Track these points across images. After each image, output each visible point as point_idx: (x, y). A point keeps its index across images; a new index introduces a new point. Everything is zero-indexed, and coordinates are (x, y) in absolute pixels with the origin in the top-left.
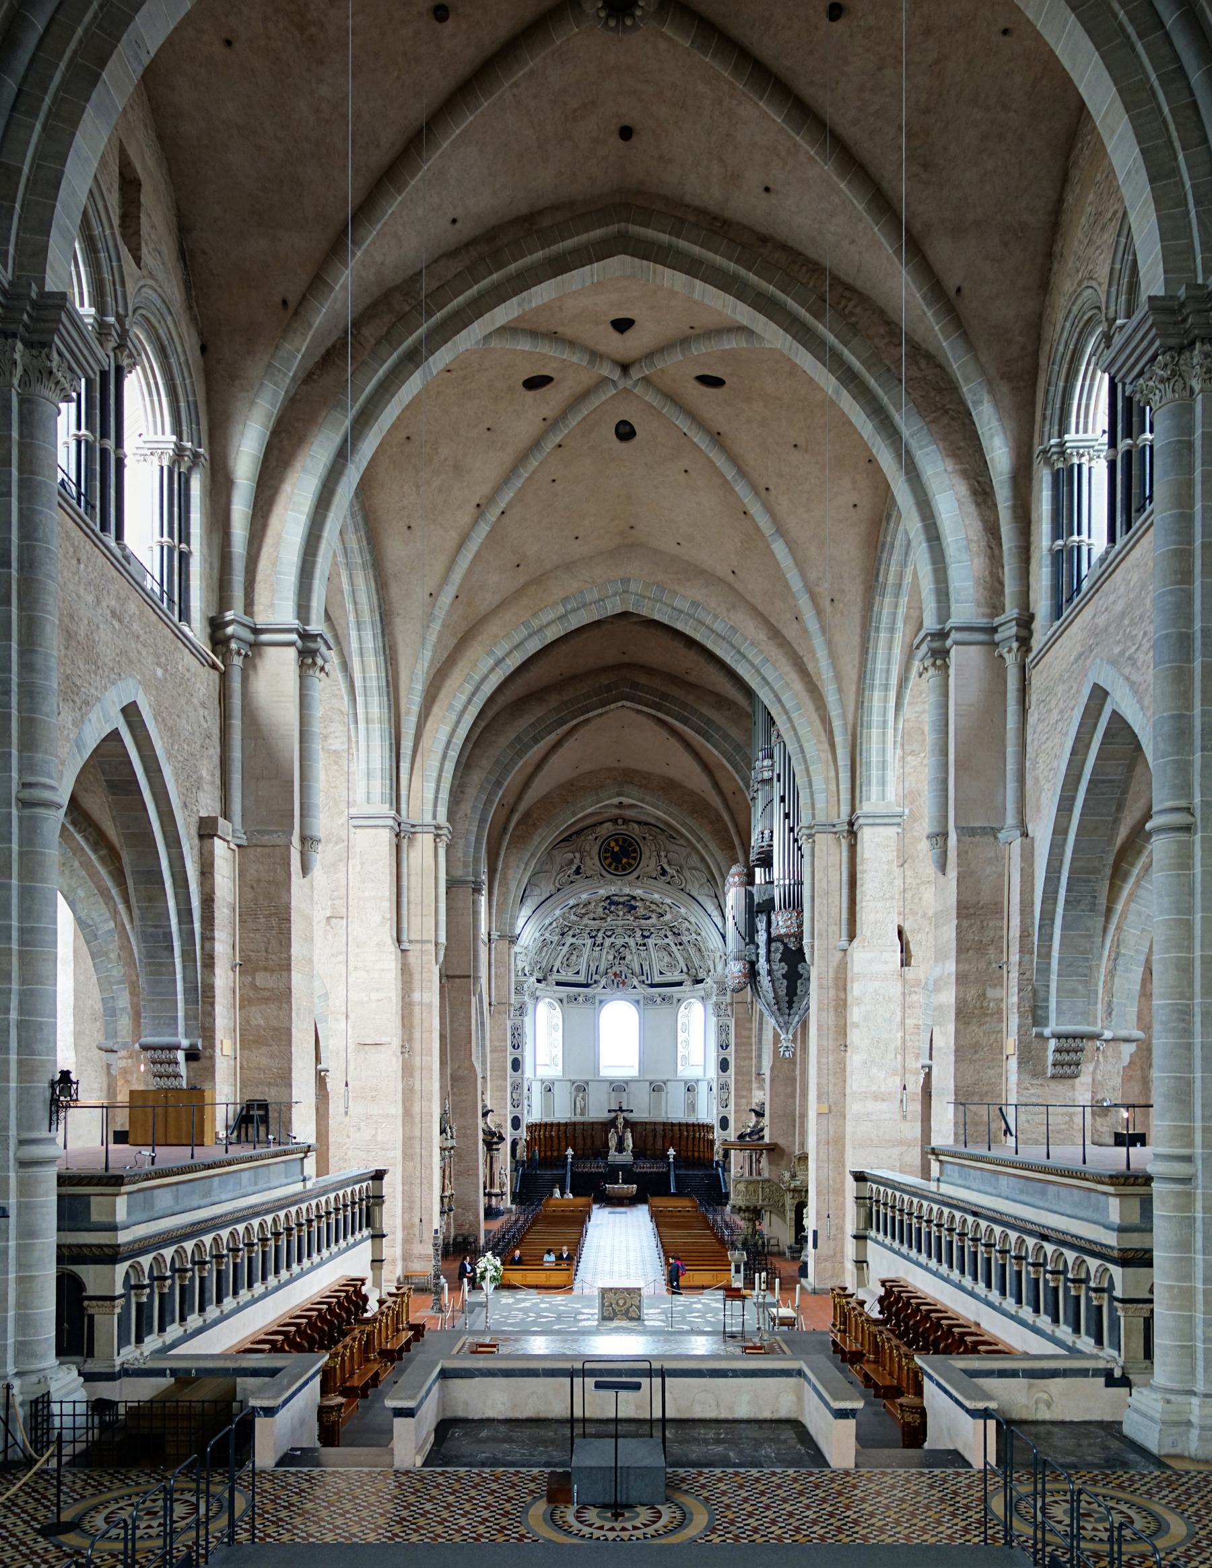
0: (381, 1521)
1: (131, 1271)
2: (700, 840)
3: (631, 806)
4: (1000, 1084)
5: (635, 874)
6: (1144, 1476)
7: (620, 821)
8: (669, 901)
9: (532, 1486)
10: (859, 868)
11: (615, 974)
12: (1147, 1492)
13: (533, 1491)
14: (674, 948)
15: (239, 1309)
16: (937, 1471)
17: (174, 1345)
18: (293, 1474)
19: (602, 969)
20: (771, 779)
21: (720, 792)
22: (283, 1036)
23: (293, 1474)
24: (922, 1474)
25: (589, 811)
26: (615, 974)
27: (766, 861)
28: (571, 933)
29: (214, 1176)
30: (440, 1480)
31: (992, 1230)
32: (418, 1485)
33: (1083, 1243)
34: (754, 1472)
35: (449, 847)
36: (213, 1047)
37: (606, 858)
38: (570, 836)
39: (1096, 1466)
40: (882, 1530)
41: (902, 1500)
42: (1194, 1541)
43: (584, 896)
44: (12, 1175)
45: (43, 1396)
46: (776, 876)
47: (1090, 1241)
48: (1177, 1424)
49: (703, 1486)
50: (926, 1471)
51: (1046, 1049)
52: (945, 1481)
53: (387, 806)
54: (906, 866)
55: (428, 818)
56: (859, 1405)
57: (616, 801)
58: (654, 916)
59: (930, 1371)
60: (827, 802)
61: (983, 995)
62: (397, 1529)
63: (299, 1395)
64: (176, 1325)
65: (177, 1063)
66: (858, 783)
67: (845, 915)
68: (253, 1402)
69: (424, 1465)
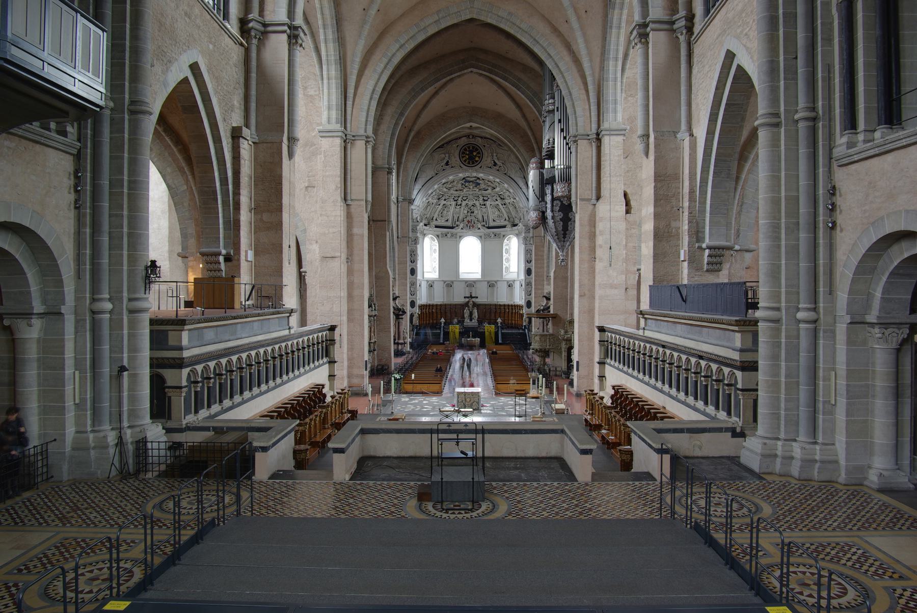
0: (324, 508)
1: (191, 373)
3: (476, 128)
5: (479, 165)
6: (751, 484)
7: (471, 137)
8: (498, 180)
9: (410, 491)
10: (602, 159)
11: (468, 222)
12: (751, 492)
13: (410, 494)
14: (501, 207)
16: (637, 483)
18: (278, 483)
19: (461, 218)
20: (554, 110)
22: (277, 249)
23: (278, 483)
24: (629, 485)
25: (453, 131)
26: (468, 222)
27: (551, 156)
28: (443, 198)
29: (238, 323)
30: (359, 487)
32: (346, 490)
33: (721, 359)
34: (535, 484)
35: (374, 149)
37: (463, 157)
38: (443, 145)
39: (725, 479)
40: (604, 513)
41: (616, 498)
42: (776, 517)
43: (451, 178)
46: (556, 163)
48: (770, 456)
49: (506, 491)
50: (631, 483)
51: (704, 255)
52: (641, 488)
53: (339, 125)
54: (628, 158)
55: (362, 132)
56: (593, 447)
57: (468, 125)
58: (490, 188)
59: (635, 429)
61: (669, 225)
62: (333, 512)
63: (282, 442)
65: (220, 263)
66: (601, 112)
67: (594, 185)
68: (255, 444)
69: (350, 480)
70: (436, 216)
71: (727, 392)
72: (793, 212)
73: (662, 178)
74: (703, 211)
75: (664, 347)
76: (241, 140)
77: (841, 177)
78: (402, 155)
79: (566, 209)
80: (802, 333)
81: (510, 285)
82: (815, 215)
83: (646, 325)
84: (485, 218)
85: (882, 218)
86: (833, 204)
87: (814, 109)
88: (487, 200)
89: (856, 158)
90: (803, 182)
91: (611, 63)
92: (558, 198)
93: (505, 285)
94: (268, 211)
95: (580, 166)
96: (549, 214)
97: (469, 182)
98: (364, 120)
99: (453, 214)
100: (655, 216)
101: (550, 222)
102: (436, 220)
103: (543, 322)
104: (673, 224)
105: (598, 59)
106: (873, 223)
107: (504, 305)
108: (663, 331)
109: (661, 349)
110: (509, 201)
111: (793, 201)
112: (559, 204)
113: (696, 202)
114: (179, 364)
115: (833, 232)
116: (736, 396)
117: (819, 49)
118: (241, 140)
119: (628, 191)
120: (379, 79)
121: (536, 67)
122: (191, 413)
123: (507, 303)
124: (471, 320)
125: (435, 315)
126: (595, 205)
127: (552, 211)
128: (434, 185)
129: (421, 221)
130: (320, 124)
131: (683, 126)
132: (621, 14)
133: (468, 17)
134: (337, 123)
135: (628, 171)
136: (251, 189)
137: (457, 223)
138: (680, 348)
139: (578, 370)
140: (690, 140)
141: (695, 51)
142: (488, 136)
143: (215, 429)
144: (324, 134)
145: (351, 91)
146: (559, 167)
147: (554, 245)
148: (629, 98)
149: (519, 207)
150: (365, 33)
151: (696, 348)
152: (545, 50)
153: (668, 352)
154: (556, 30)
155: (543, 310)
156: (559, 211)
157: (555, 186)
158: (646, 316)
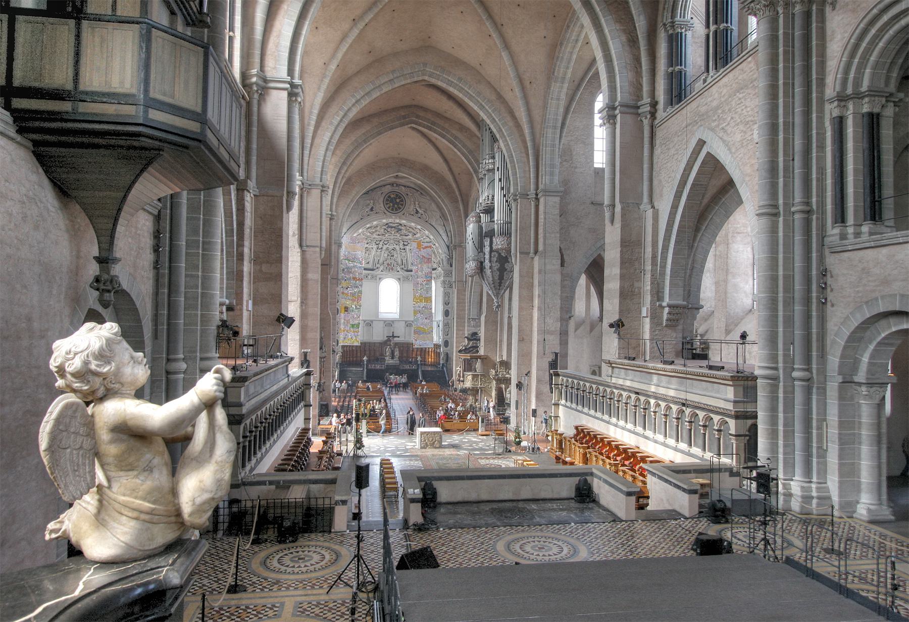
2: (440, 197)
5: (403, 212)
8: (419, 227)
11: (388, 264)
19: (381, 261)
26: (388, 264)
27: (489, 211)
36: (242, 304)
46: (496, 218)
55: (318, 181)
58: (411, 235)
67: (532, 241)
72: (789, 288)
73: (627, 244)
74: (663, 274)
75: (637, 393)
76: (246, 192)
79: (503, 260)
82: (808, 291)
85: (877, 299)
87: (808, 203)
89: (850, 248)
90: (798, 264)
91: (550, 131)
92: (497, 251)
94: (268, 262)
96: (487, 264)
97: (392, 227)
100: (621, 277)
101: (488, 272)
104: (636, 285)
106: (867, 303)
109: (633, 396)
111: (788, 279)
112: (497, 255)
115: (824, 306)
117: (814, 155)
118: (246, 192)
120: (335, 131)
121: (473, 127)
124: (393, 358)
125: (355, 352)
126: (533, 258)
127: (490, 261)
128: (359, 229)
131: (646, 199)
132: (562, 87)
133: (420, 78)
137: (377, 265)
139: (517, 408)
141: (657, 134)
145: (308, 141)
148: (564, 163)
150: (324, 87)
157: (494, 239)
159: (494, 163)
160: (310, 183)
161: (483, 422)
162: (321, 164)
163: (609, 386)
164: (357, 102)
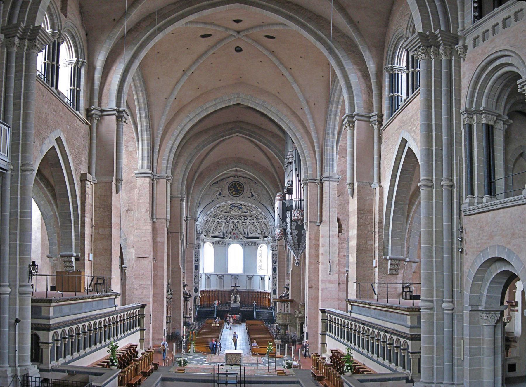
1: (55, 334)
2: (266, 184)
4: (372, 276)
5: (242, 196)
8: (254, 206)
11: (234, 234)
15: (91, 352)
17: (70, 362)
19: (229, 231)
20: (292, 162)
21: (274, 167)
26: (234, 234)
27: (290, 192)
28: (217, 217)
31: (369, 330)
37: (231, 190)
38: (217, 182)
43: (222, 204)
44: (17, 297)
45: (26, 374)
47: (401, 332)
53: (149, 169)
54: (340, 196)
57: (234, 169)
60: (313, 171)
64: (70, 356)
67: (318, 213)
70: (212, 229)
71: (403, 354)
72: (440, 241)
75: (363, 324)
76: (86, 182)
77: (465, 220)
78: (191, 188)
79: (300, 228)
80: (445, 317)
81: (262, 279)
83: (352, 309)
84: (246, 231)
86: (462, 238)
88: (247, 220)
92: (295, 220)
93: (259, 278)
95: (310, 199)
96: (289, 230)
98: (165, 166)
99: (224, 228)
102: (212, 232)
103: (284, 305)
104: (369, 242)
105: (322, 133)
107: (258, 292)
108: (363, 314)
109: (362, 326)
110: (262, 220)
111: (440, 234)
112: (296, 224)
113: (383, 229)
114: (48, 328)
116: (408, 356)
118: (86, 182)
119: (340, 218)
121: (281, 134)
122: (54, 360)
123: (259, 291)
127: (291, 229)
129: (202, 233)
130: (136, 169)
131: (376, 180)
134: (147, 168)
135: (340, 205)
136: (92, 213)
138: (373, 325)
139: (307, 339)
140: (379, 189)
142: (247, 176)
143: (68, 371)
144: (139, 175)
146: (296, 199)
147: (292, 252)
149: (269, 225)
151: (384, 325)
152: (287, 125)
153: (366, 328)
154: (294, 113)
155: (284, 297)
156: (295, 229)
157: (293, 212)
158: (352, 303)
159: (292, 158)
160: (158, 175)
161: (278, 348)
162: (166, 162)
163: (347, 319)
164: (190, 120)
